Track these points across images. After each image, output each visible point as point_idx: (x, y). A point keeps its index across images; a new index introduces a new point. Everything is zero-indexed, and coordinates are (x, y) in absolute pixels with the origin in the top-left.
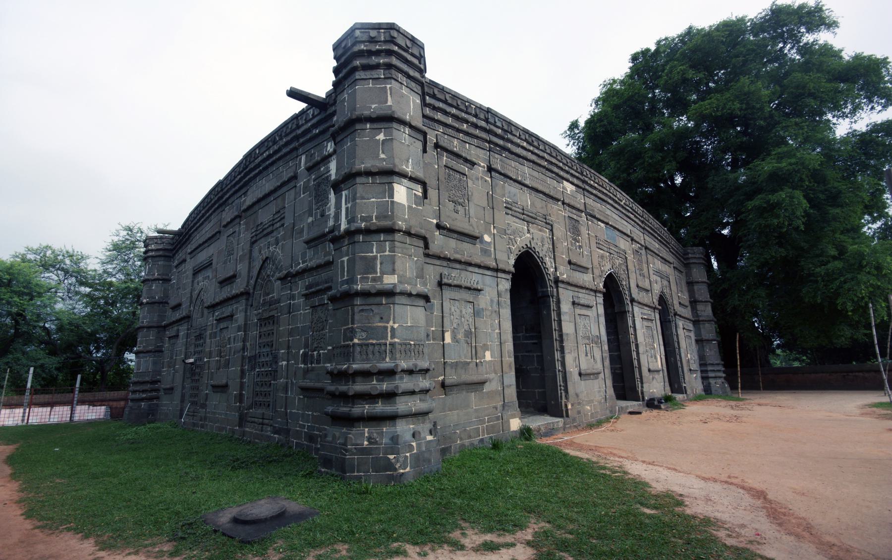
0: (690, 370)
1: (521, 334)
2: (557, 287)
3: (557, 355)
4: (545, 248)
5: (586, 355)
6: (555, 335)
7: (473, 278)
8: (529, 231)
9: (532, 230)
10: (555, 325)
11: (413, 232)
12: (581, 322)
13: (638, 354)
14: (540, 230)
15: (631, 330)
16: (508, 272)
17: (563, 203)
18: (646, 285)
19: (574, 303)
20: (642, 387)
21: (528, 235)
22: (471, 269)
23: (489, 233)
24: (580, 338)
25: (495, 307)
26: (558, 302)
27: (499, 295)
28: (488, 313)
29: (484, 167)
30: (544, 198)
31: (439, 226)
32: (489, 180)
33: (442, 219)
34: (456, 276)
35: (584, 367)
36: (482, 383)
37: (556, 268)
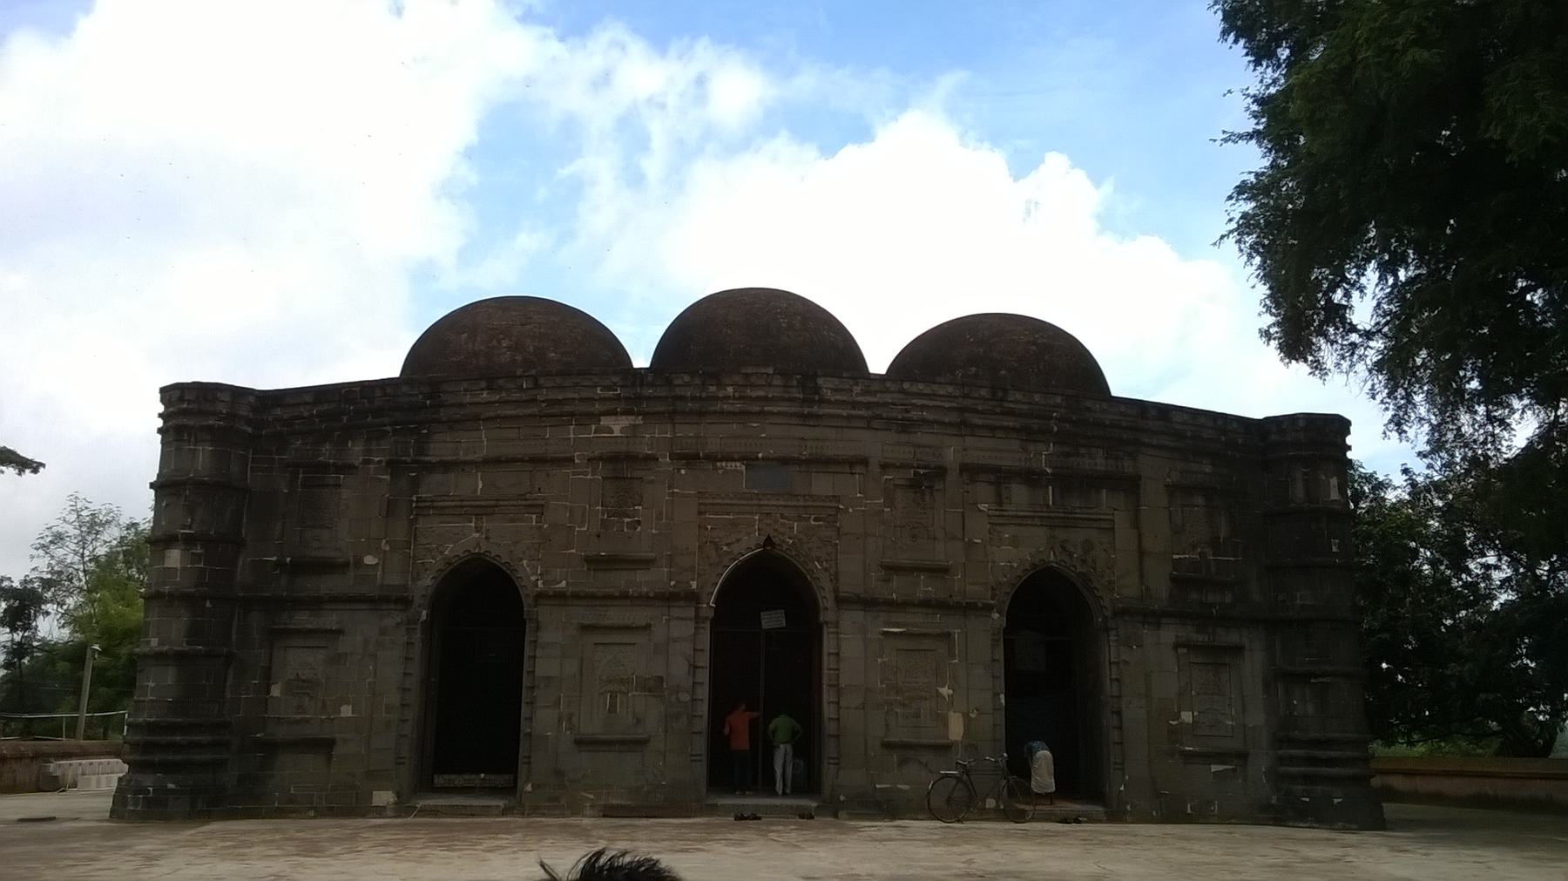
7: (330, 620)
14: (512, 520)
26: (538, 629)
27: (383, 632)
29: (380, 462)
34: (303, 620)
36: (331, 743)
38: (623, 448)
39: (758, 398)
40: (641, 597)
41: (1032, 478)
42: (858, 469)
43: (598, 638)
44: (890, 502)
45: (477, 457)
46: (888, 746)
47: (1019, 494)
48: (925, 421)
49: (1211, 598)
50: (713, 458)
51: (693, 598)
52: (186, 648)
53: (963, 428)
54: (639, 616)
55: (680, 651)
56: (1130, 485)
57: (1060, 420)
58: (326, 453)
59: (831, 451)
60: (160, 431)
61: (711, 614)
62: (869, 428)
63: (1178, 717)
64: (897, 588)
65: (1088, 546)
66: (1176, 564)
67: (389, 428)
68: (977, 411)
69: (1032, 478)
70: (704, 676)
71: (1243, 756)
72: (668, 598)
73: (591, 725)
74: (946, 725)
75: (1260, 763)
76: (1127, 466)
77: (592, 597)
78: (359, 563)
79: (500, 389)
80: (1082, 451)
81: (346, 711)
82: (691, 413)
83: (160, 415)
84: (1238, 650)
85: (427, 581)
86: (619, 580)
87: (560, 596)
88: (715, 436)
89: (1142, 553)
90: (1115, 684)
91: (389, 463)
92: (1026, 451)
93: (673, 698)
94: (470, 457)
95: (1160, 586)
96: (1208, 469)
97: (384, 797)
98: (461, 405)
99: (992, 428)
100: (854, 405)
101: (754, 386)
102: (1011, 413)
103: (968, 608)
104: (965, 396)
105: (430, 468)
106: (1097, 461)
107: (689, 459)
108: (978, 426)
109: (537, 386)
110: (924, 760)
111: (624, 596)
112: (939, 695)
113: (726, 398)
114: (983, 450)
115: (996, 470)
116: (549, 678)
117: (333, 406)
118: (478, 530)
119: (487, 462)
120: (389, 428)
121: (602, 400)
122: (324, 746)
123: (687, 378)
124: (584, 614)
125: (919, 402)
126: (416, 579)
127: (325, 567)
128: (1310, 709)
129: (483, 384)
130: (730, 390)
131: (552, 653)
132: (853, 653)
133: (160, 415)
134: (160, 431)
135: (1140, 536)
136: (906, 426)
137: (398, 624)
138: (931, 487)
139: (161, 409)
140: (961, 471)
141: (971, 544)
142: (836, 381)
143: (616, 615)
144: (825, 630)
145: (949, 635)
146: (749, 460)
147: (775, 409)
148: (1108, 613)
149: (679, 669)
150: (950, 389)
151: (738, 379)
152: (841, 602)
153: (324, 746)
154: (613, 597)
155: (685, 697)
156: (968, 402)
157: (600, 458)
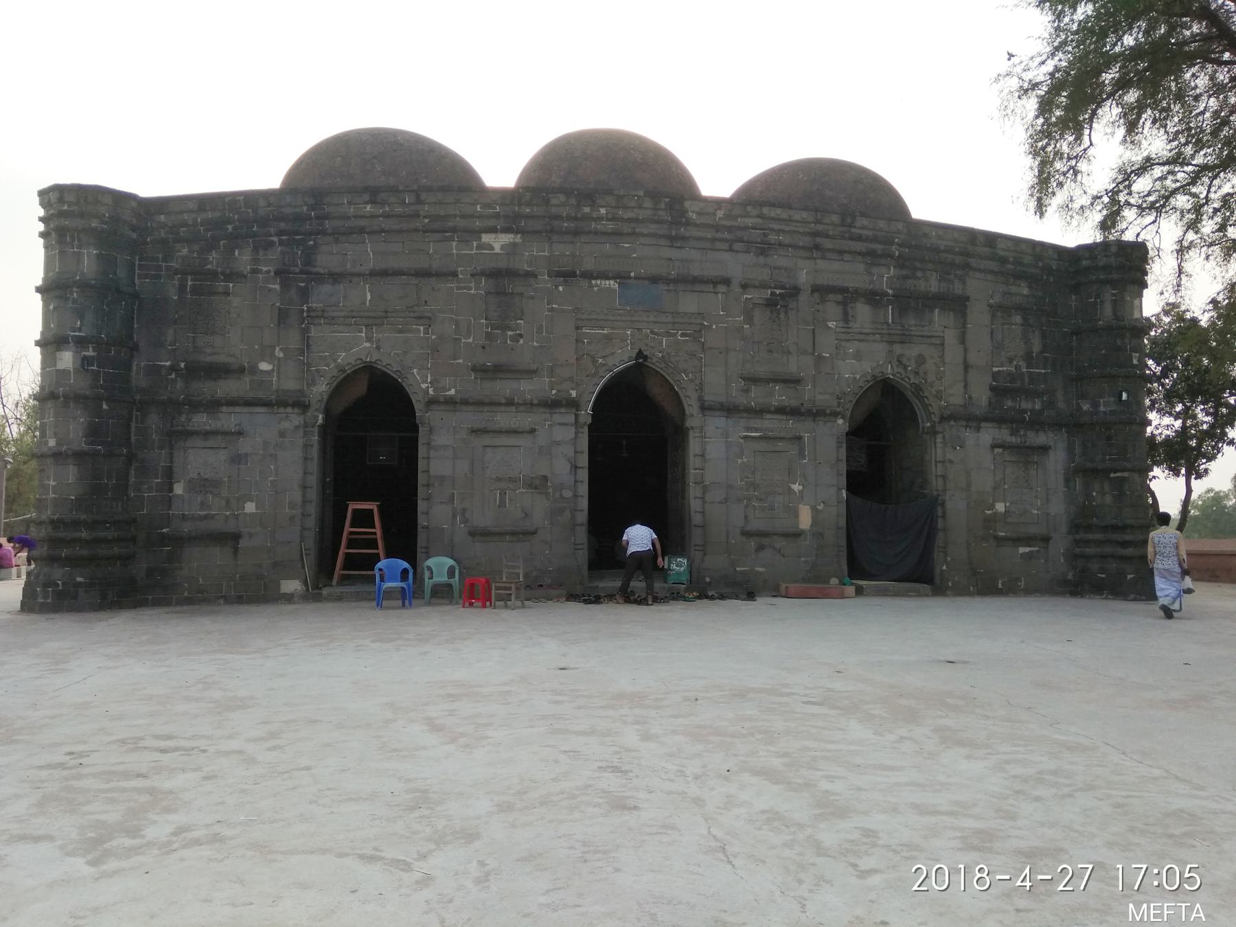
7: (229, 420)
14: (400, 332)
21: (368, 345)
22: (224, 409)
23: (271, 358)
26: (431, 431)
27: (282, 434)
29: (268, 272)
30: (414, 280)
31: (173, 368)
32: (277, 287)
34: (201, 420)
36: (236, 537)
38: (503, 264)
39: (630, 220)
40: (524, 404)
41: (874, 298)
42: (722, 288)
43: (487, 440)
44: (749, 319)
46: (747, 534)
47: (863, 311)
49: (1025, 405)
50: (589, 276)
51: (574, 404)
52: (85, 447)
53: (815, 250)
54: (524, 420)
55: (560, 454)
56: (957, 305)
57: (900, 245)
58: (214, 259)
59: (695, 271)
60: (42, 235)
61: (589, 421)
62: (731, 250)
63: (992, 507)
64: (756, 396)
65: (921, 360)
66: (995, 376)
67: (275, 239)
68: (828, 236)
69: (874, 298)
70: (584, 475)
71: (1046, 540)
72: (552, 405)
73: (484, 518)
74: (797, 516)
75: (1060, 545)
76: (957, 288)
77: (479, 403)
78: (254, 370)
79: (383, 203)
80: (919, 274)
81: (250, 507)
82: (567, 232)
83: (41, 219)
84: (1045, 449)
85: (321, 389)
86: (504, 388)
87: (450, 402)
88: (589, 254)
89: (966, 367)
90: (940, 480)
92: (870, 274)
93: (557, 495)
94: (358, 269)
95: (982, 396)
96: (1025, 291)
97: (291, 586)
98: (346, 218)
99: (841, 252)
100: (717, 228)
101: (625, 207)
102: (859, 238)
103: (817, 414)
104: (817, 222)
105: (320, 278)
107: (567, 275)
108: (829, 250)
109: (419, 201)
111: (510, 403)
112: (790, 490)
113: (600, 218)
114: (833, 271)
115: (843, 290)
116: (442, 477)
117: (217, 214)
118: (369, 339)
119: (373, 274)
120: (275, 239)
121: (481, 217)
123: (562, 198)
124: (469, 418)
125: (776, 227)
126: (314, 383)
127: (219, 371)
128: (1108, 499)
129: (366, 197)
130: (603, 211)
131: (443, 453)
132: (715, 456)
133: (41, 219)
134: (42, 235)
135: (966, 350)
136: (764, 249)
137: (297, 427)
138: (785, 306)
139: (41, 212)
140: (813, 292)
141: (820, 357)
143: (504, 419)
144: (691, 432)
145: (799, 438)
146: (621, 277)
147: (645, 231)
148: (936, 419)
149: (560, 469)
150: (805, 214)
151: (610, 200)
152: (705, 408)
153: (230, 539)
154: (500, 404)
155: (568, 494)
156: (820, 227)
157: (483, 273)
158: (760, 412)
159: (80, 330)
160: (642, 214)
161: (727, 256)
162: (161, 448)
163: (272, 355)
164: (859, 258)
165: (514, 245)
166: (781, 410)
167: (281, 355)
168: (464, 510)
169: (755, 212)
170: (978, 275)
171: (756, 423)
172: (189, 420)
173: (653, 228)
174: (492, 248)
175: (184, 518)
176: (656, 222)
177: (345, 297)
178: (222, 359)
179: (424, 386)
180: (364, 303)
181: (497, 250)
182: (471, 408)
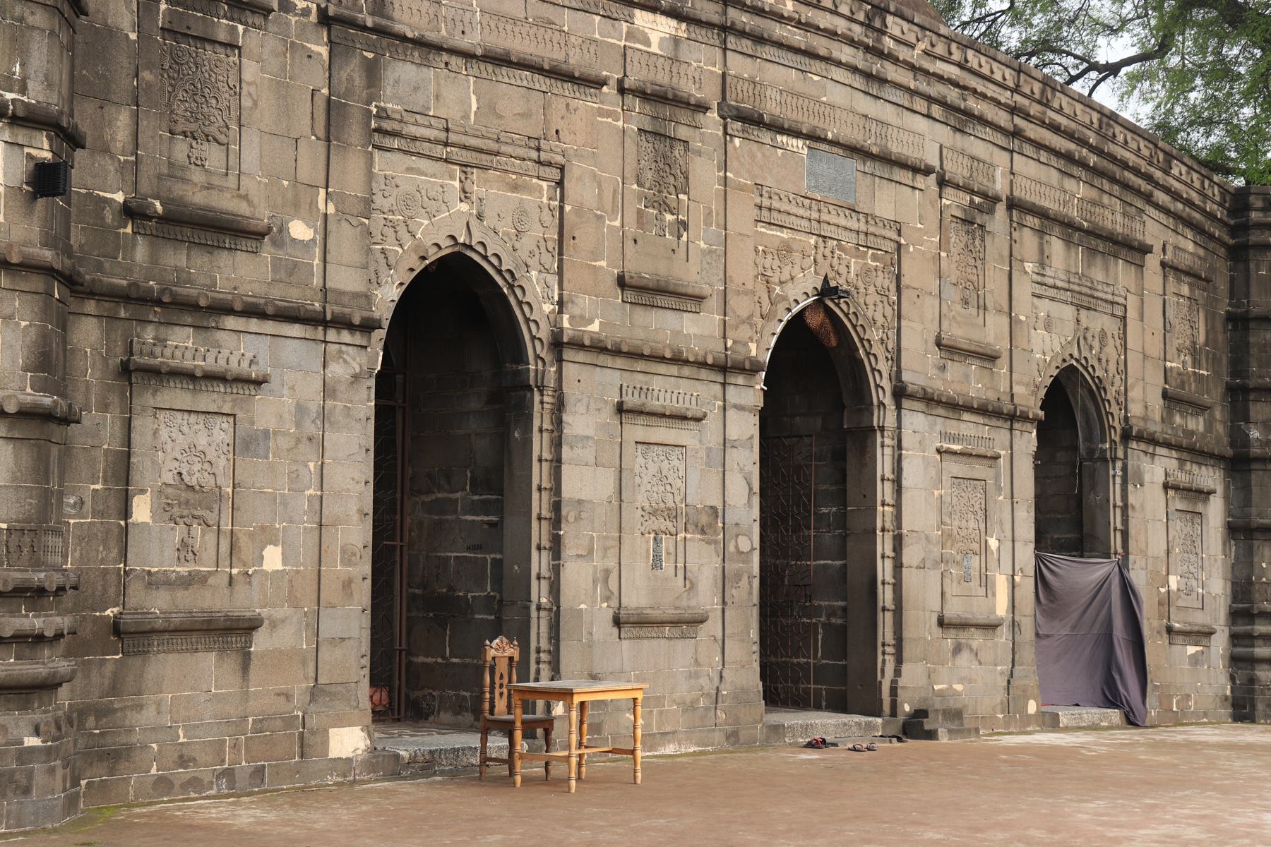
0: (1170, 630)
1: (458, 495)
2: (560, 360)
3: (539, 563)
4: (526, 244)
5: (657, 564)
6: (539, 504)
8: (465, 195)
9: (476, 190)
10: (539, 474)
11: (15, 260)
12: (644, 467)
13: (898, 566)
14: (515, 188)
15: (884, 492)
16: (368, 326)
17: (622, 90)
18: (993, 332)
19: (620, 409)
20: (898, 673)
21: (464, 207)
22: (231, 322)
24: (633, 517)
25: (311, 429)
26: (560, 405)
27: (328, 391)
28: (284, 443)
29: (306, 12)
30: (541, 82)
31: (130, 212)
32: (323, 51)
33: (145, 187)
34: (182, 345)
35: (636, 598)
36: (248, 627)
37: (561, 303)
38: (663, 78)
42: (920, 181)
43: (663, 433)
45: (473, 40)
48: (982, 121)
59: (895, 148)
68: (1027, 116)
69: (1068, 227)
72: (726, 368)
75: (1220, 643)
84: (1203, 494)
85: (388, 295)
88: (774, 82)
89: (1145, 357)
91: (325, 19)
96: (1190, 247)
99: (1039, 146)
102: (1055, 128)
103: (1013, 417)
104: (1016, 90)
106: (1113, 218)
110: (975, 644)
111: (678, 360)
115: (1042, 214)
116: (580, 502)
118: (465, 195)
122: (232, 632)
125: (991, 90)
136: (962, 119)
137: (356, 377)
142: (906, 25)
143: (667, 389)
153: (232, 632)
157: (642, 94)
158: (955, 407)
159: (23, 90)
160: (841, 25)
161: (921, 124)
162: (104, 407)
163: (313, 204)
164: (1054, 161)
165: (676, 41)
166: (984, 410)
167: (331, 209)
168: (607, 572)
169: (957, 56)
170: (1154, 213)
171: (953, 427)
172: (161, 341)
173: (846, 54)
174: (648, 44)
175: (153, 582)
176: (852, 42)
177: (437, 97)
178: (226, 203)
179: (547, 308)
180: (466, 117)
181: (655, 49)
182: (620, 362)
